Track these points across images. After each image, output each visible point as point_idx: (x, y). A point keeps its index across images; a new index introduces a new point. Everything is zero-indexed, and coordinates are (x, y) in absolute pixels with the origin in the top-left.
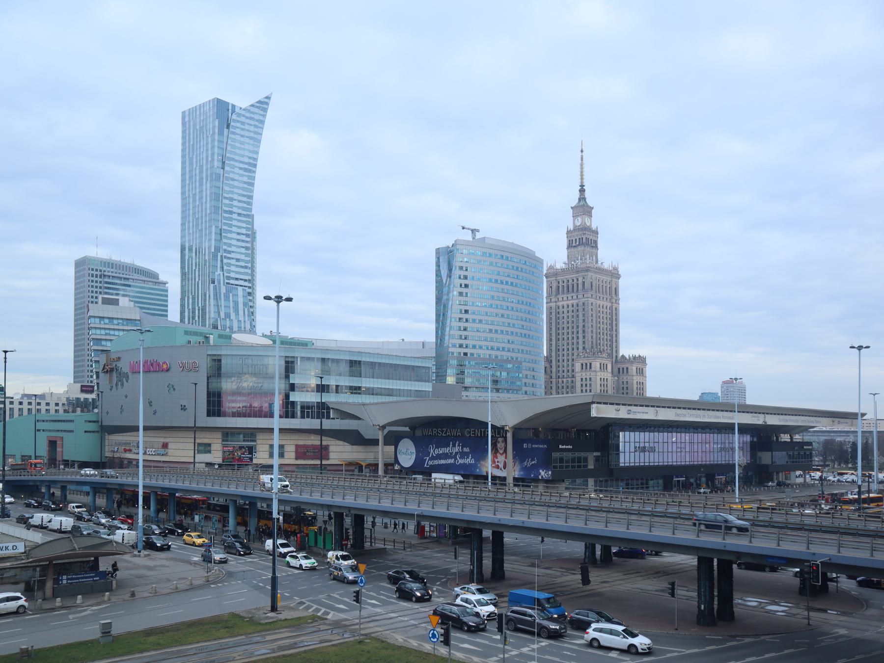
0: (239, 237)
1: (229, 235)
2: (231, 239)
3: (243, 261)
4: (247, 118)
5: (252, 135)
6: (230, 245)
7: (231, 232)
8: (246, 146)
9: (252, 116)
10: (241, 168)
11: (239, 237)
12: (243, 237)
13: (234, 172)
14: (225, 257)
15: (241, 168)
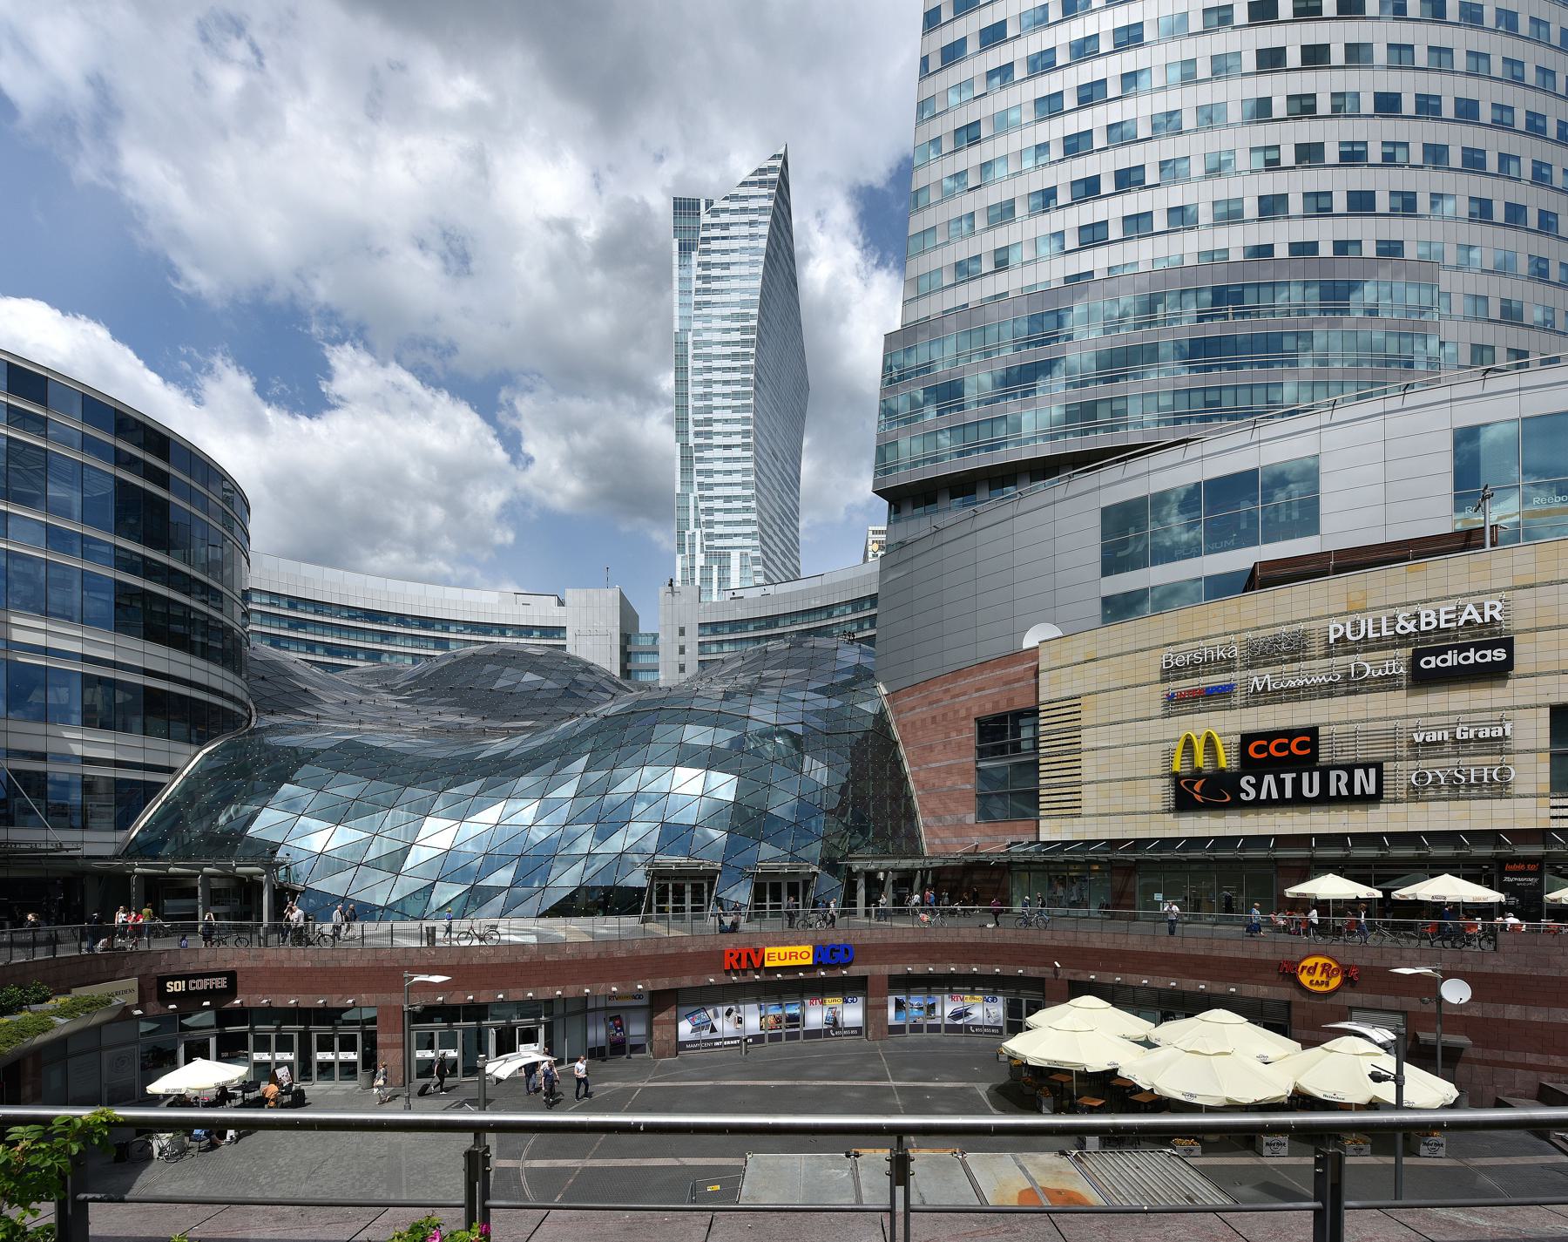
1: (707, 454)
2: (710, 460)
3: (737, 498)
6: (709, 473)
7: (710, 447)
11: (728, 453)
12: (737, 452)
14: (702, 497)
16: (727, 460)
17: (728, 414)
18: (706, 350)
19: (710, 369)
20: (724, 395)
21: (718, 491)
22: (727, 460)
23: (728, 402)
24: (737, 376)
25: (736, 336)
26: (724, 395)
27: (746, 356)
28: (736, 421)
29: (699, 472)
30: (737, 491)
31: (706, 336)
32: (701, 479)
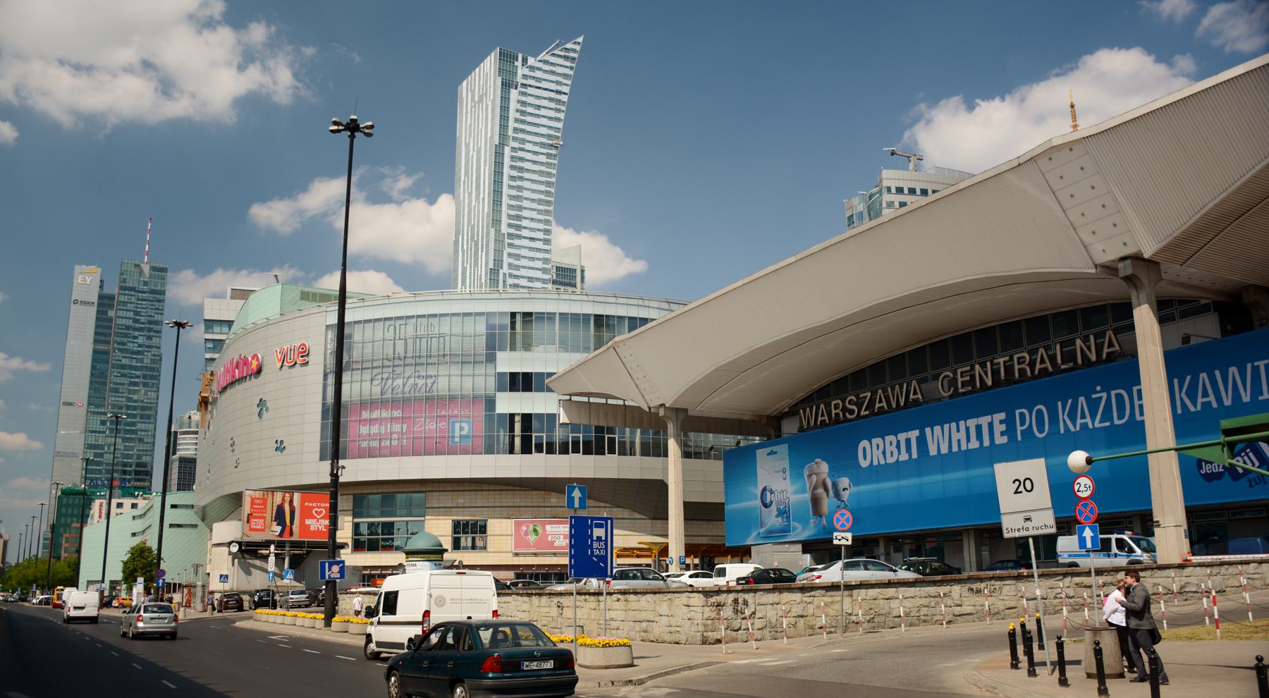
0: (532, 244)
1: (516, 242)
3: (538, 279)
4: (545, 71)
5: (553, 95)
6: (518, 257)
7: (519, 237)
8: (543, 112)
9: (553, 68)
10: (535, 143)
11: (532, 244)
13: (522, 150)
14: (510, 275)
15: (535, 143)
16: (531, 249)
17: (534, 215)
18: (520, 164)
19: (521, 178)
20: (533, 200)
21: (523, 272)
22: (531, 249)
23: (534, 206)
24: (542, 188)
25: (543, 159)
26: (533, 200)
27: (549, 174)
28: (540, 221)
29: (510, 255)
30: (539, 274)
31: (521, 154)
32: (511, 261)
